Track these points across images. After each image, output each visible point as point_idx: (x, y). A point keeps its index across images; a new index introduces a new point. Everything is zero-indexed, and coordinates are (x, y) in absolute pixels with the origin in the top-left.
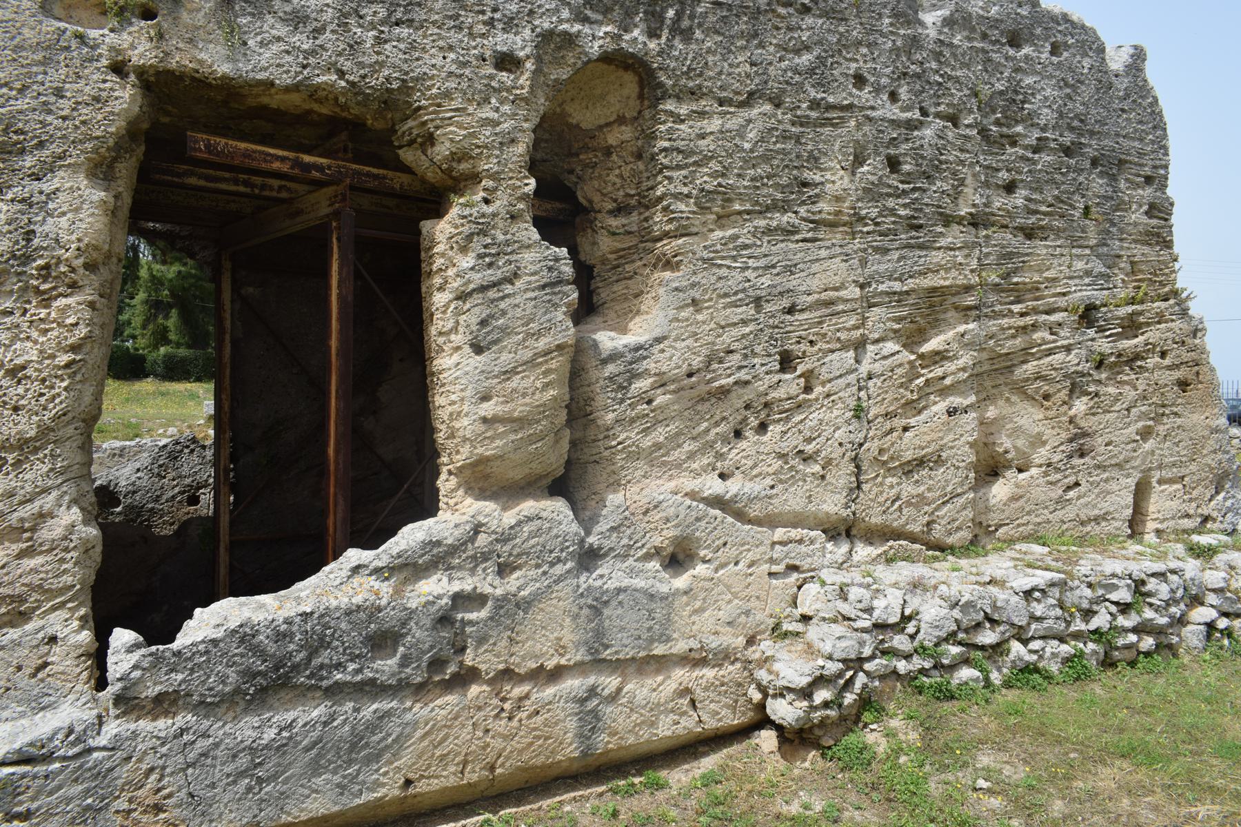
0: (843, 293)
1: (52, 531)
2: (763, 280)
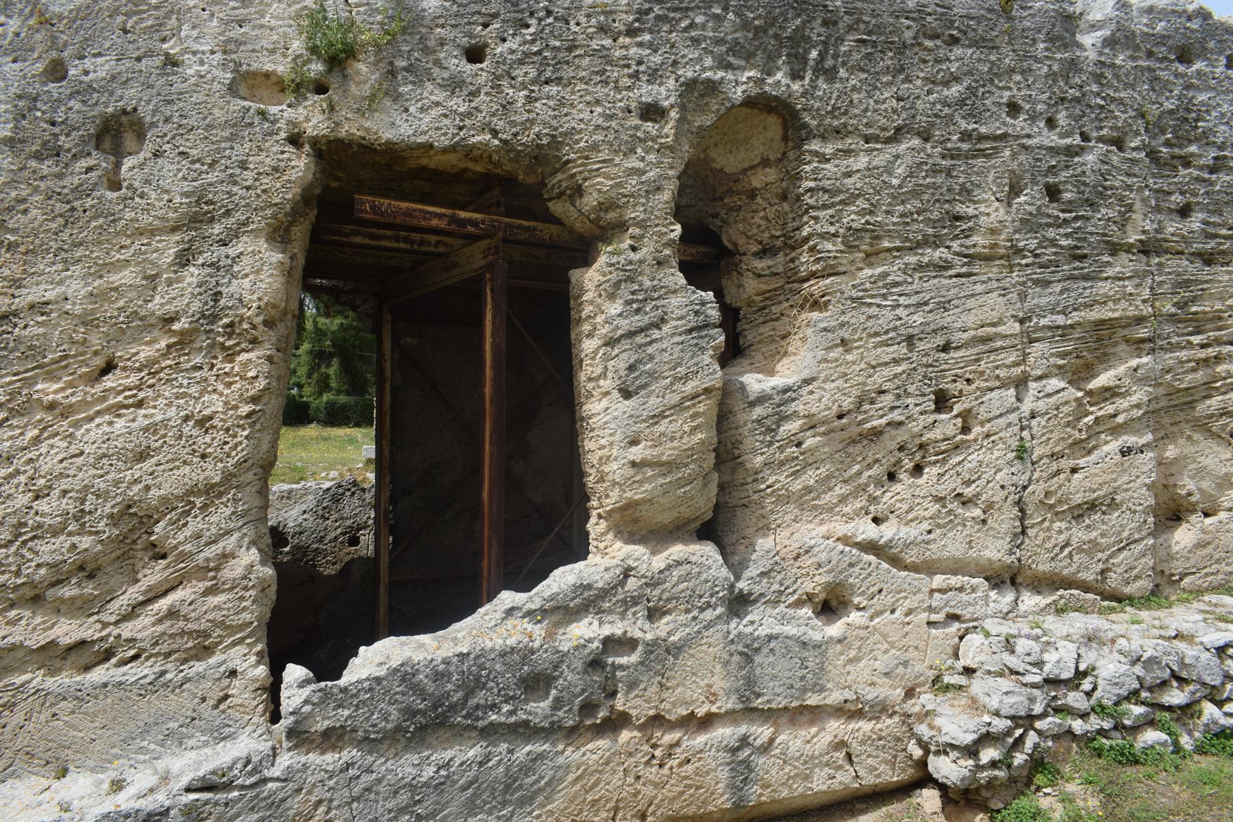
0: (1001, 329)
2: (915, 317)
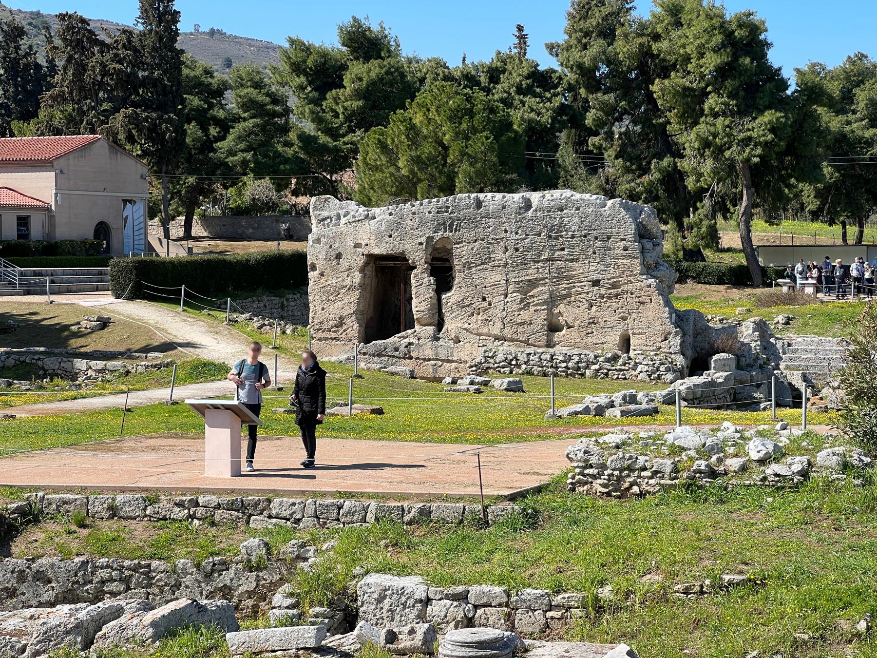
1: (355, 327)
